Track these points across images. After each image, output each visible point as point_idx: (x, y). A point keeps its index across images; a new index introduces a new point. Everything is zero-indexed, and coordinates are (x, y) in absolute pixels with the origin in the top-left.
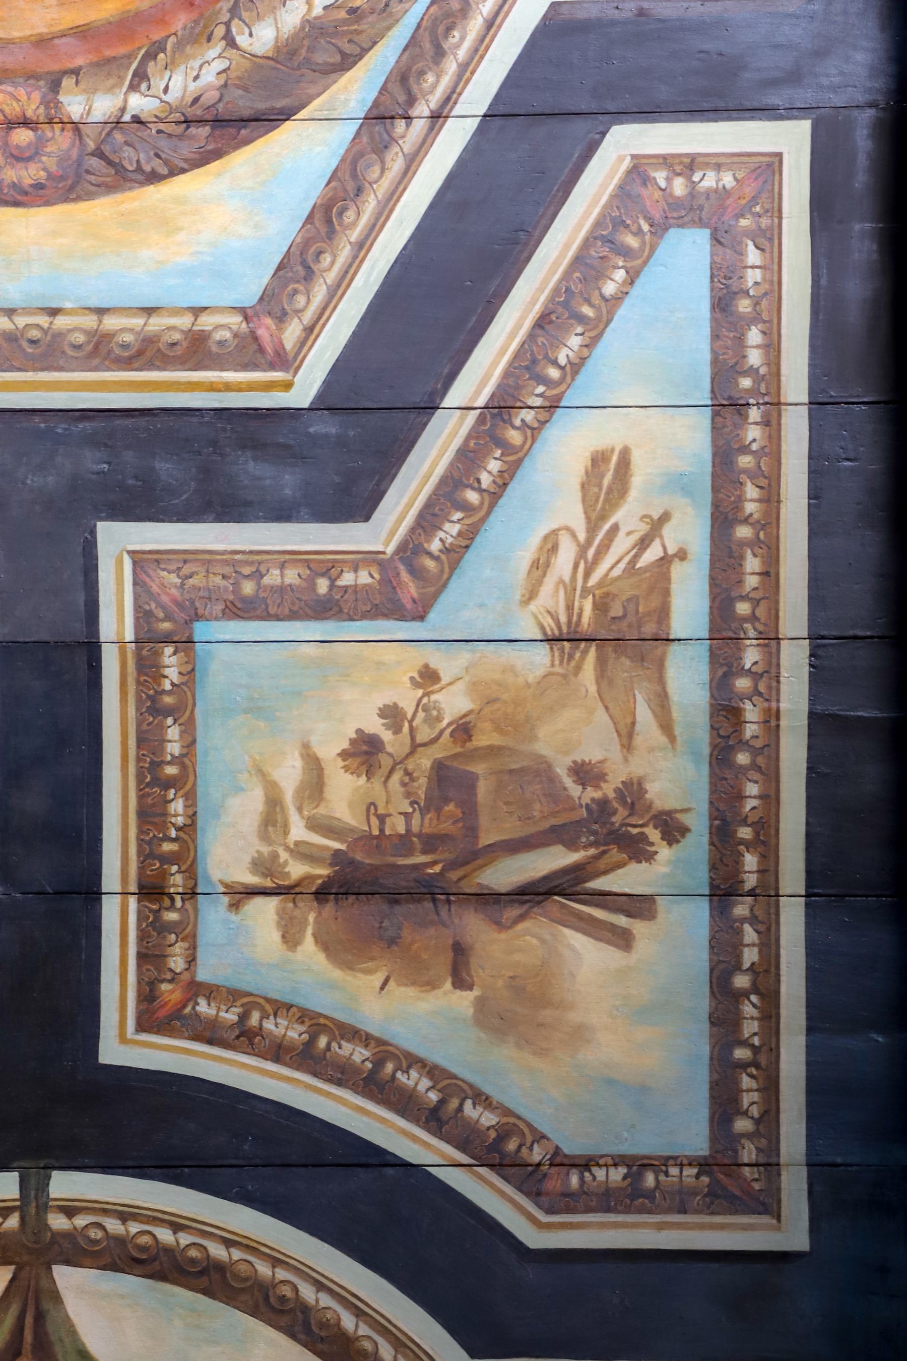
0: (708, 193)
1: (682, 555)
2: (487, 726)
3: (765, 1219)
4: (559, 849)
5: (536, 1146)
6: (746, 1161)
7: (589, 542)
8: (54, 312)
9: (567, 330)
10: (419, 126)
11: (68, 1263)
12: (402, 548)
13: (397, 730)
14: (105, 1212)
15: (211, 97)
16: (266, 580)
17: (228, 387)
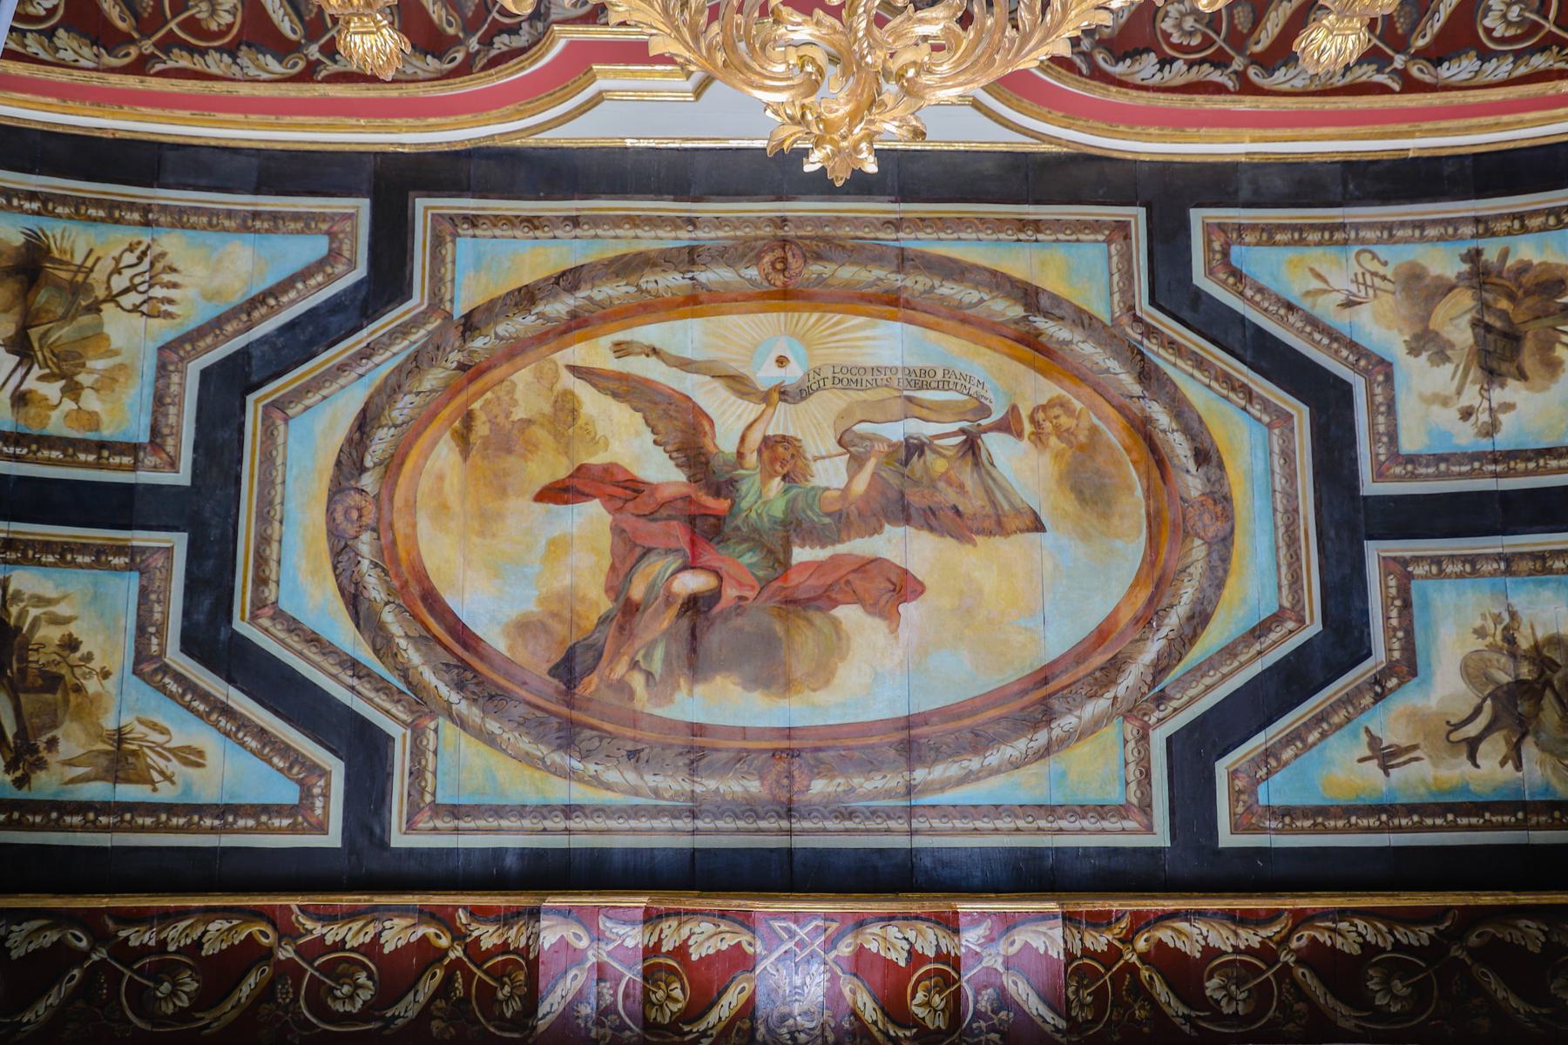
0: (313, 803)
1: (155, 790)
2: (79, 700)
4: (15, 729)
7: (165, 749)
8: (281, 522)
9: (259, 741)
10: (350, 681)
12: (167, 666)
13: (80, 659)
15: (366, 594)
16: (156, 605)
17: (244, 593)
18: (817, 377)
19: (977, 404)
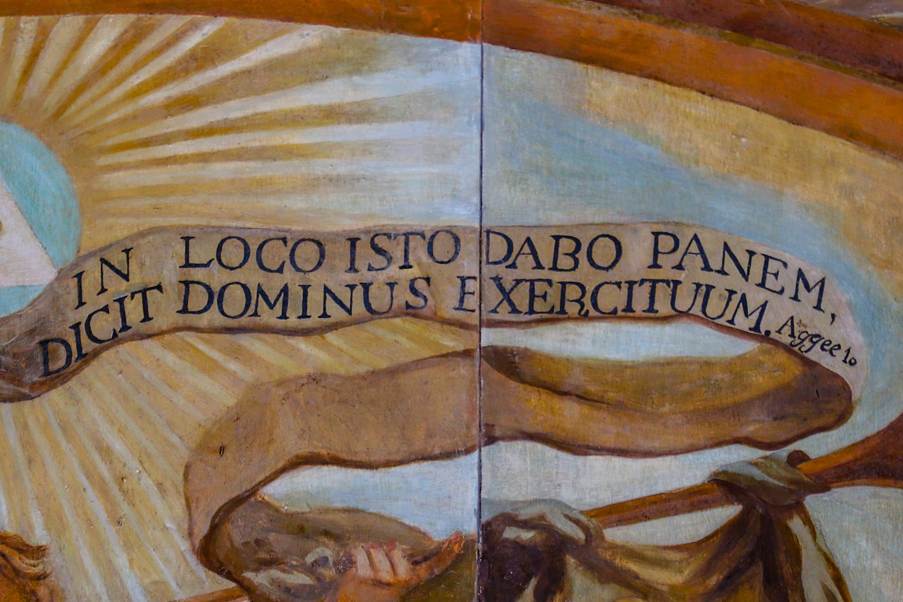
18: (117, 286)
19: (794, 369)
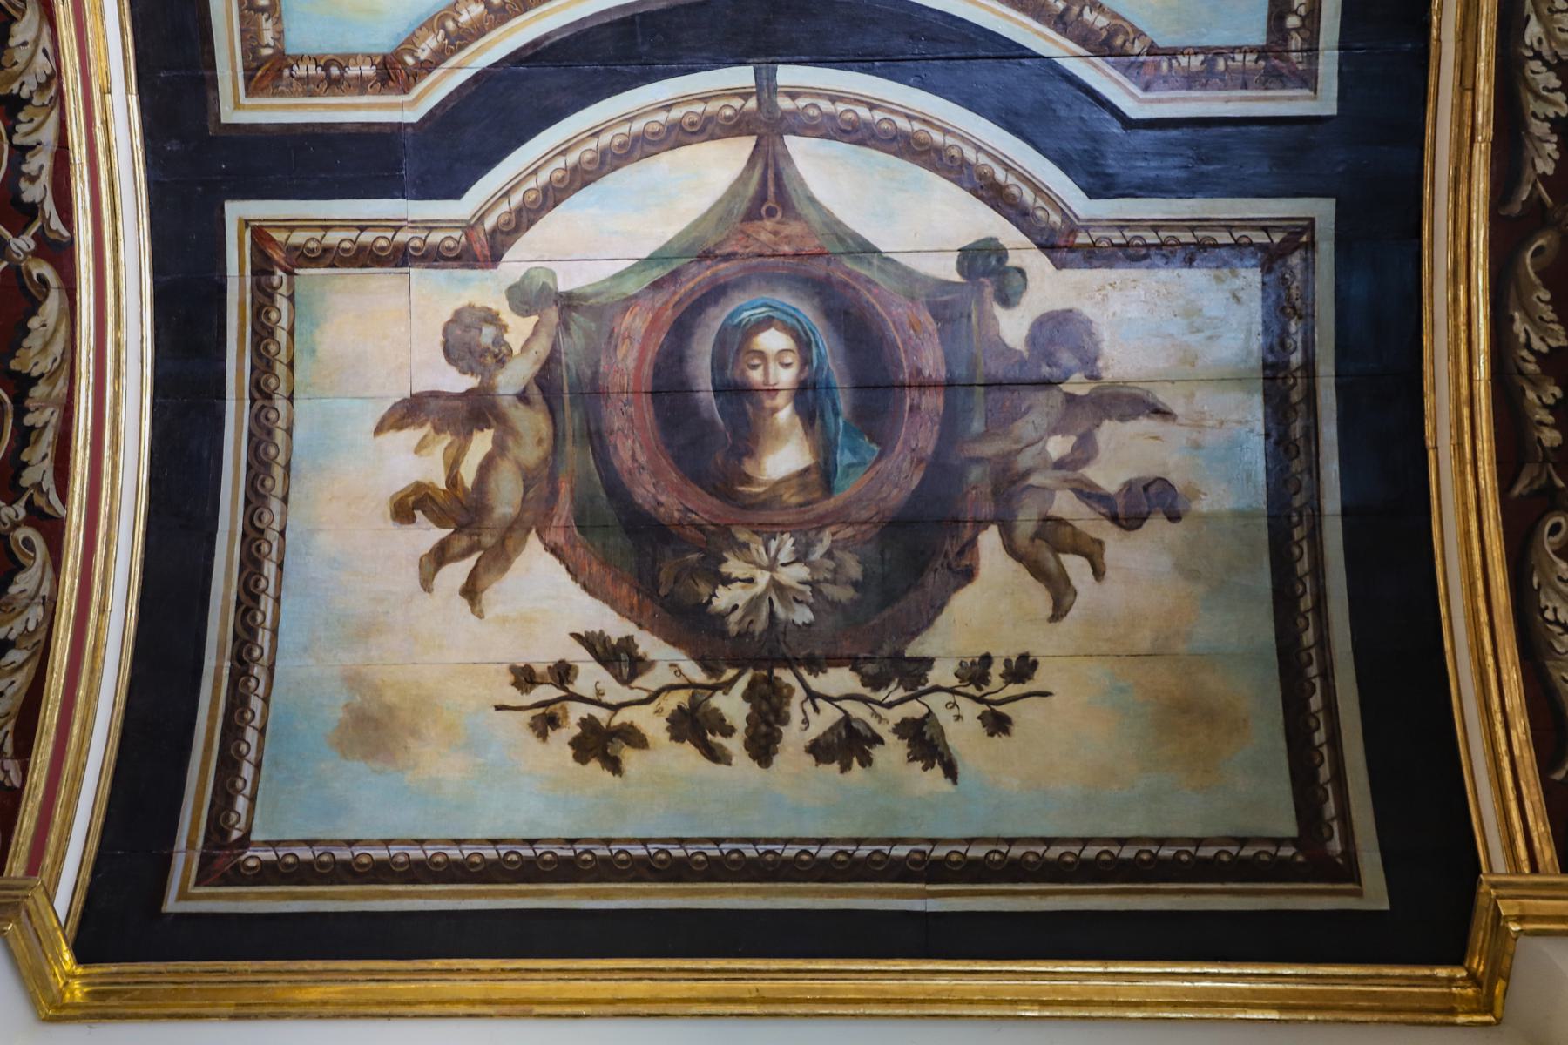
3: (1306, 92)
5: (1136, 41)
6: (1293, 48)
11: (795, 133)
14: (819, 96)
